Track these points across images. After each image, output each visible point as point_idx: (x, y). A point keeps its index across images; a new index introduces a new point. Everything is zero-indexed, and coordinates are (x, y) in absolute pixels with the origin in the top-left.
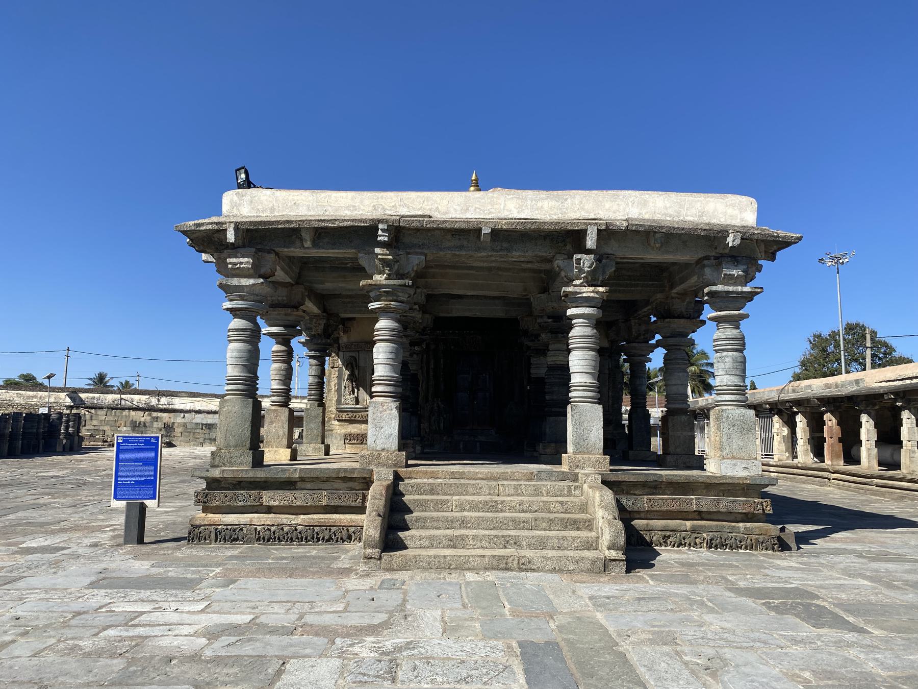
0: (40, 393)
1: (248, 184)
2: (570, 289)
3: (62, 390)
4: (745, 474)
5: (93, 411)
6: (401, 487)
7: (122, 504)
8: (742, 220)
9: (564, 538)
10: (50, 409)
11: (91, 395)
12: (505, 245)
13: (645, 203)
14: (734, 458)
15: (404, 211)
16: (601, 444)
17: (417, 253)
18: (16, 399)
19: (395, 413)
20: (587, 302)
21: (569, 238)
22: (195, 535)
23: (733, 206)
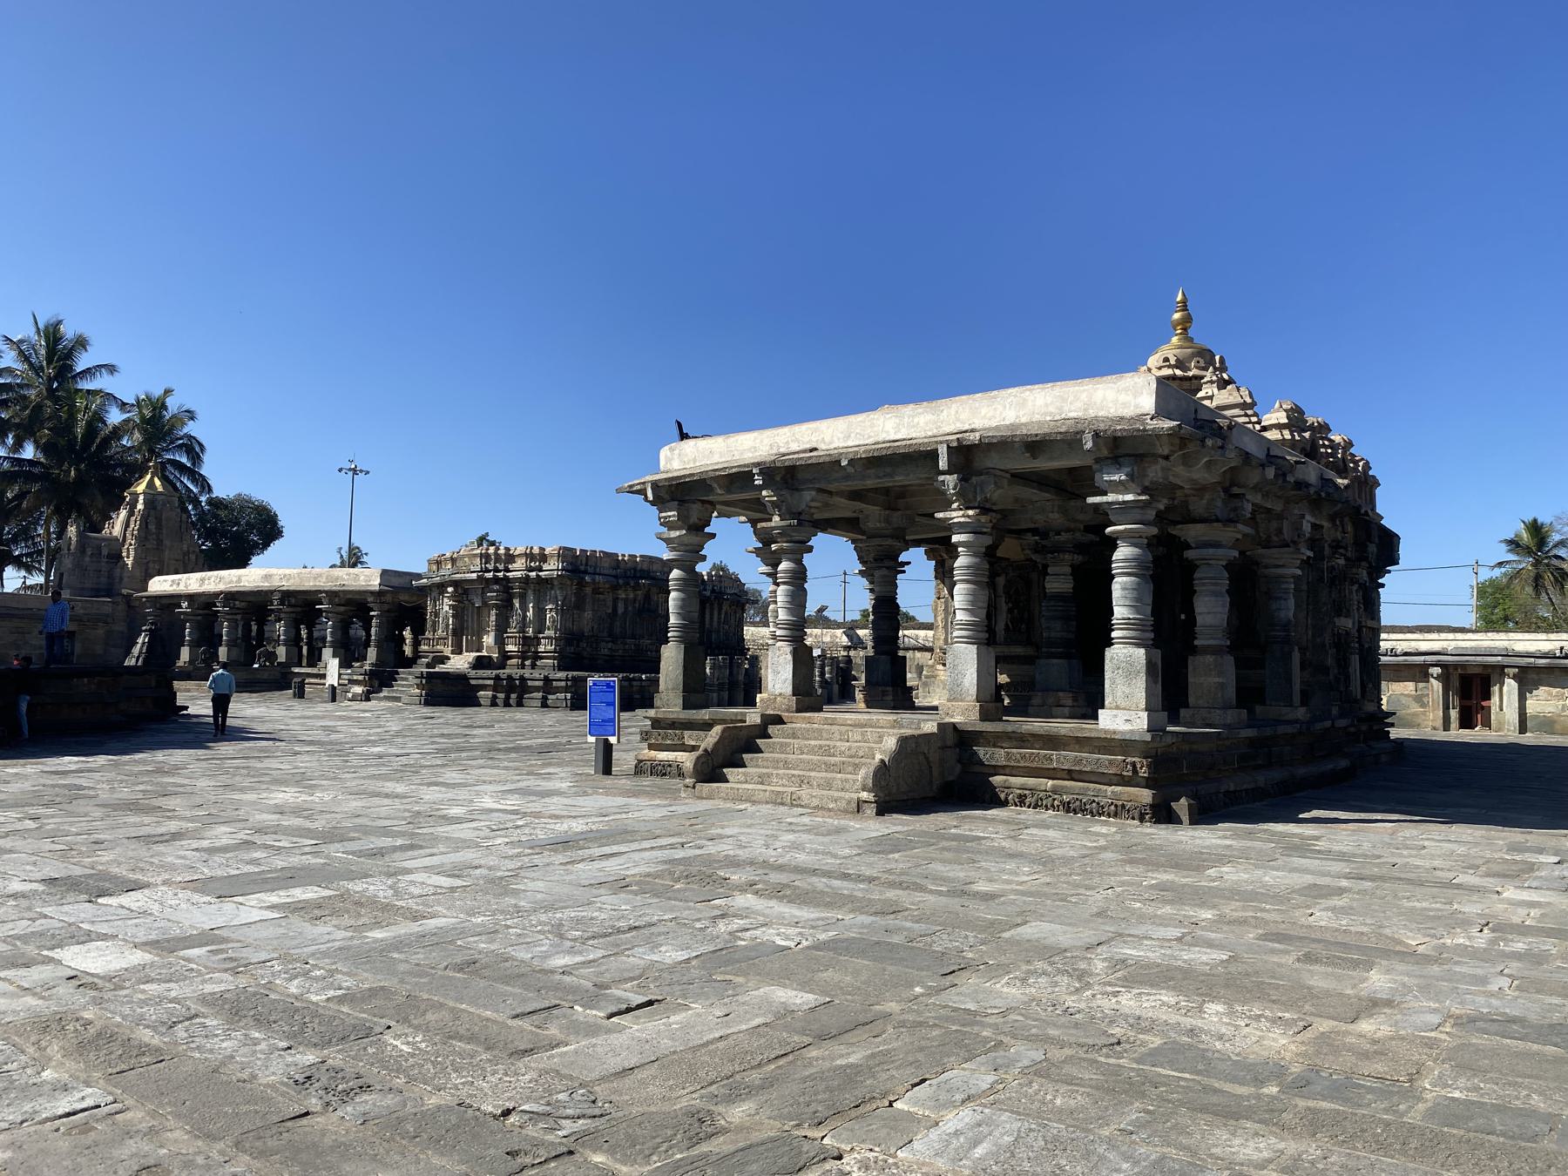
1: (684, 436)
2: (940, 515)
3: (838, 625)
4: (1127, 727)
6: (771, 729)
7: (592, 739)
8: (1136, 406)
9: (847, 780)
12: (888, 470)
13: (1023, 403)
14: (1117, 708)
15: (795, 447)
16: (973, 691)
17: (809, 489)
19: (790, 657)
20: (962, 528)
21: (921, 457)
22: (640, 769)
23: (1126, 390)
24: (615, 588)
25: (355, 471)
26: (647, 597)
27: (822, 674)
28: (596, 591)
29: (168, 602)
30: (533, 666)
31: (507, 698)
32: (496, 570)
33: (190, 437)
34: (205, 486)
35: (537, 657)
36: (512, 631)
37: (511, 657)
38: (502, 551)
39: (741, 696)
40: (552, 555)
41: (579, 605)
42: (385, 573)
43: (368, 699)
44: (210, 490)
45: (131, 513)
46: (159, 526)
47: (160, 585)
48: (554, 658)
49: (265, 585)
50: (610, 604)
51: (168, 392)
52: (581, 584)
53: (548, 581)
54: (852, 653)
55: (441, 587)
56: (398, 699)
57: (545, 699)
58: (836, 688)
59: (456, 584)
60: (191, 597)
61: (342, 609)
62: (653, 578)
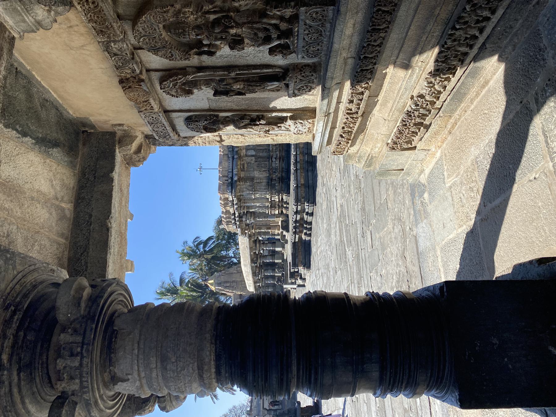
24: (240, 157)
28: (243, 170)
31: (306, 228)
33: (194, 242)
34: (210, 238)
37: (282, 211)
41: (252, 179)
46: (226, 282)
57: (307, 214)
60: (255, 283)
61: (258, 245)
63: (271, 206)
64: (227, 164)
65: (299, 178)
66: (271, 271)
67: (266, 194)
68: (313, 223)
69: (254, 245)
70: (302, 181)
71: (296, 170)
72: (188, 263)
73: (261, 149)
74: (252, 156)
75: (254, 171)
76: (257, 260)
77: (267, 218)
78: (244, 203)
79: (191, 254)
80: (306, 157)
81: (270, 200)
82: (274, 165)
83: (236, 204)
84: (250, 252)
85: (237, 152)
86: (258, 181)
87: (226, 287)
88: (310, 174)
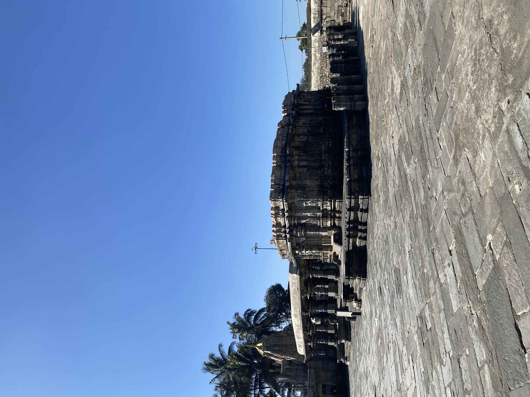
0: (313, 52)
5: (324, 17)
10: (324, 46)
11: (312, 19)
18: (317, 66)
24: (292, 167)
25: (256, 248)
26: (297, 148)
27: (339, 40)
28: (295, 178)
29: (308, 349)
30: (340, 212)
31: (361, 231)
32: (285, 232)
33: (245, 314)
35: (334, 210)
36: (319, 223)
37: (334, 223)
38: (275, 229)
39: (357, 87)
40: (275, 204)
41: (303, 188)
42: (291, 271)
43: (360, 301)
44: (264, 308)
45: (272, 355)
46: (275, 346)
47: (301, 350)
48: (335, 202)
49: (299, 317)
50: (301, 170)
51: (228, 323)
52: (291, 187)
53: (289, 206)
54: (324, 29)
55: (295, 255)
56: (361, 290)
57: (362, 210)
58: (347, 31)
59: (293, 249)
60: (306, 342)
61: (309, 288)
62: (286, 145)
63: (322, 215)
64: (279, 173)
65: (352, 173)
66: (323, 327)
67: (318, 201)
68: (369, 222)
69: (305, 288)
70: (356, 177)
71: (349, 167)
72: (238, 336)
73: (313, 160)
74: (304, 167)
75: (306, 179)
76: (308, 308)
77: (319, 231)
78: (295, 212)
79: (241, 326)
80: (360, 153)
81: (321, 209)
82: (326, 173)
83: (287, 212)
84: (301, 296)
85: (290, 161)
86: (309, 189)
87: (275, 351)
88: (363, 168)
